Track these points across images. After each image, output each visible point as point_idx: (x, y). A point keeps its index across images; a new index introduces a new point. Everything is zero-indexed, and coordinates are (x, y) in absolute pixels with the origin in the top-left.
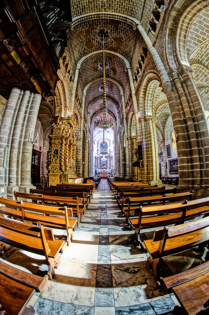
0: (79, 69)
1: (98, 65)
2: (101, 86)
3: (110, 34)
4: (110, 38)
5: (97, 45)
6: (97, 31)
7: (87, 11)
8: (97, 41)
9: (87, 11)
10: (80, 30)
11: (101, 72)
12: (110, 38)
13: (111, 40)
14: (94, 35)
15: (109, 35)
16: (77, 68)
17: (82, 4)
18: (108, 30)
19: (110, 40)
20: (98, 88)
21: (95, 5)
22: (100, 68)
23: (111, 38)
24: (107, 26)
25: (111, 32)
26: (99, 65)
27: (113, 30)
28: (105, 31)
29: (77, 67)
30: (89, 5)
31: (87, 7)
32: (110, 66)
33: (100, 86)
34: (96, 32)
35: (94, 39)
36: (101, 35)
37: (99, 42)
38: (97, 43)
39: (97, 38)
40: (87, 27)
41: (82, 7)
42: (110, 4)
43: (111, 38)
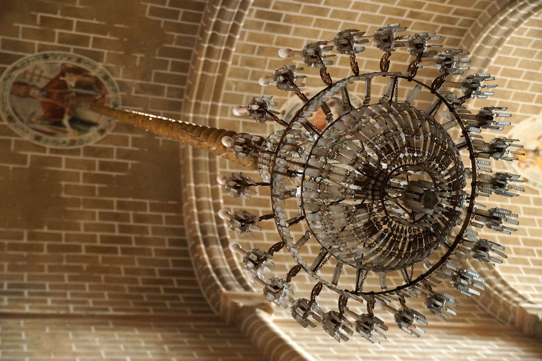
3: (73, 142)
4: (38, 138)
6: (100, 65)
13: (21, 145)
15: (68, 139)
18: (102, 132)
19: (27, 138)
23: (44, 149)
25: (89, 151)
27: (104, 166)
28: (90, 115)
31: (269, 41)
34: (97, 57)
36: (64, 85)
39: (46, 57)
41: (288, 19)
43: (44, 149)
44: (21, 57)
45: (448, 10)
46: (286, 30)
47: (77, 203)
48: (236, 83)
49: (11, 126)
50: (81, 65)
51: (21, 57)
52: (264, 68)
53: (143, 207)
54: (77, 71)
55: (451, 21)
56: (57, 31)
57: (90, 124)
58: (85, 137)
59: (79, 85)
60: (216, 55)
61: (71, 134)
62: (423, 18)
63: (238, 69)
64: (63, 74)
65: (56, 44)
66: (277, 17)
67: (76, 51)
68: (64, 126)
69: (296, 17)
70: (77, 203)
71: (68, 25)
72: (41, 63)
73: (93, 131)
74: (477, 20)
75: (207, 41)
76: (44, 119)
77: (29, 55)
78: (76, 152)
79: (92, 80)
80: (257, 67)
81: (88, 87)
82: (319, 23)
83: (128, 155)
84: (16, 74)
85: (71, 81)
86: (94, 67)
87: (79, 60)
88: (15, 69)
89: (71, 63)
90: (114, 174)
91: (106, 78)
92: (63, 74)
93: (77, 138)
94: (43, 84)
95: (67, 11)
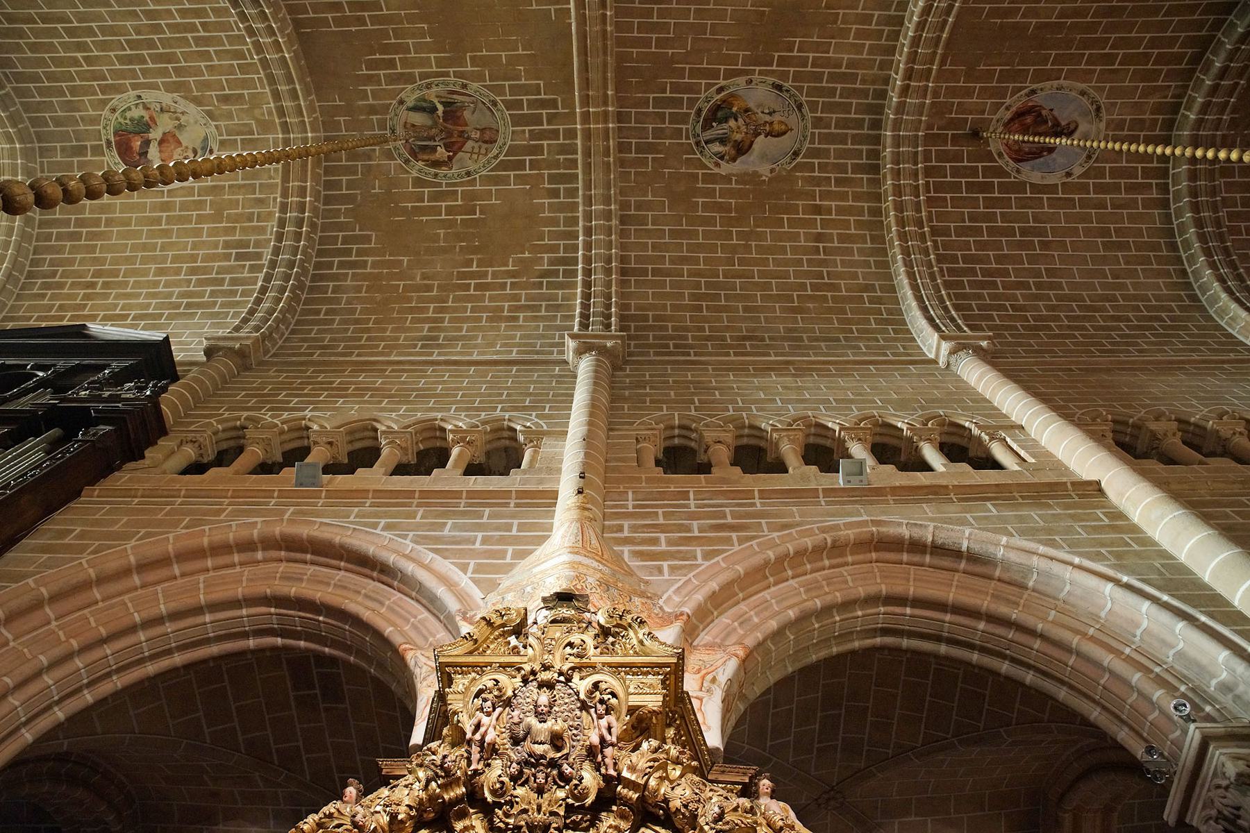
0: (953, 352)
1: (727, 179)
2: (1007, 163)
3: (429, 86)
4: (464, 86)
5: (520, 179)
6: (415, 174)
8: (488, 180)
10: (358, 289)
11: (814, 153)
12: (464, 86)
13: (479, 77)
14: (435, 197)
15: (435, 89)
16: (942, 362)
18: (401, 102)
19: (475, 85)
20: (1020, 187)
21: (240, 187)
22: (764, 157)
23: (456, 75)
24: (372, 110)
25: (410, 79)
26: (726, 168)
27: (391, 64)
28: (419, 119)
29: (935, 362)
30: (229, 219)
31: (243, 229)
32: (730, 74)
33: (1000, 172)
34: (419, 182)
35: (471, 197)
36: (448, 147)
37: (504, 166)
38: (505, 180)
39: (468, 174)
40: (367, 239)
41: (227, 257)
42: (225, 99)
43: (456, 75)
44: (492, 170)
45: (53, 297)
46: (227, 245)
47: (410, 19)
48: (270, 178)
49: (493, 96)
50: (433, 170)
51: (492, 170)
53: (338, 22)
54: (436, 164)
55: (46, 286)
56: (460, 203)
57: (415, 109)
58: (417, 94)
59: (434, 149)
60: (294, 206)
61: (432, 95)
62: (80, 283)
64: (450, 158)
65: (460, 189)
66: (239, 257)
67: (440, 185)
68: (441, 103)
69: (219, 261)
70: (410, 19)
71: (450, 211)
72: (471, 168)
73: (410, 102)
74: (17, 291)
76: (463, 108)
77: (483, 173)
78: (424, 76)
79: (420, 156)
81: (424, 149)
82: (193, 258)
83: (369, 79)
84: (495, 152)
85: (441, 153)
86: (420, 171)
87: (436, 175)
88: (496, 157)
89: (443, 171)
90: (378, 56)
91: (407, 161)
92: (450, 158)
93: (425, 92)
94: (470, 144)
95: (452, 224)
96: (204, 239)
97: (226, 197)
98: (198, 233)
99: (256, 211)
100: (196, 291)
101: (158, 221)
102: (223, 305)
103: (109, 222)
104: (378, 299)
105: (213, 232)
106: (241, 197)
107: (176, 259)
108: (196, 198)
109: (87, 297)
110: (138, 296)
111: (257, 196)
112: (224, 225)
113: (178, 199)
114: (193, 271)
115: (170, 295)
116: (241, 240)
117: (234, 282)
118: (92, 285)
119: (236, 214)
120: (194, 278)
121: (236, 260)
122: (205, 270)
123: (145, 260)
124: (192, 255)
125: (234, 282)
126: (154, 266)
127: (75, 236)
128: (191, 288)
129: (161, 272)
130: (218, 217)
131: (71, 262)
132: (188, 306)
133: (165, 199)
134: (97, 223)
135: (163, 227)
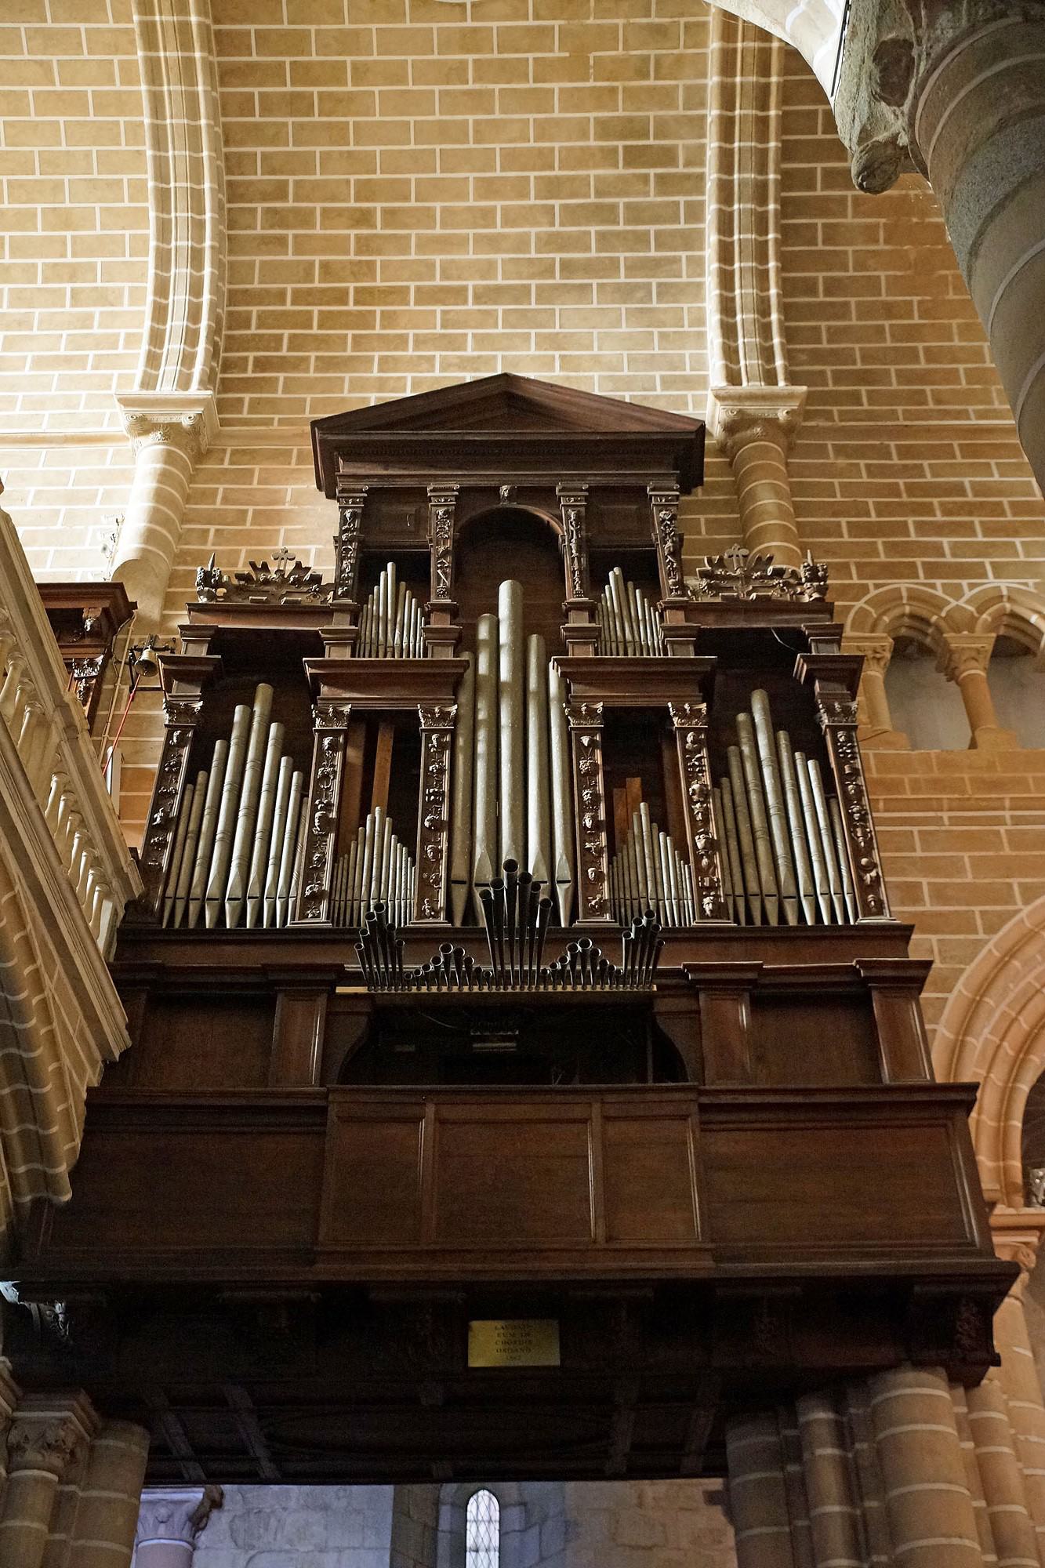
7: (666, 97)
9: (666, 97)
10: (870, 233)
17: (583, 158)
46: (605, 129)
52: (625, 26)
55: (276, 218)
60: (749, 60)
62: (340, 212)
63: (682, 15)
66: (634, 157)
69: (596, 166)
75: (774, 90)
80: (642, 27)
82: (543, 159)
96: (556, 114)
97: (591, 21)
98: (541, 100)
99: (653, 53)
100: (570, 235)
101: (457, 72)
102: (634, 267)
103: (361, 73)
104: (912, 256)
105: (572, 99)
106: (620, 22)
107: (512, 159)
108: (531, 22)
109: (364, 244)
110: (460, 243)
111: (654, 20)
112: (591, 84)
113: (494, 24)
114: (551, 188)
115: (522, 244)
116: (630, 120)
117: (636, 214)
118: (363, 218)
119: (613, 60)
120: (557, 203)
121: (628, 164)
122: (575, 187)
123: (450, 161)
124: (540, 151)
125: (636, 214)
126: (472, 176)
127: (298, 104)
128: (557, 228)
129: (488, 188)
130: (576, 67)
131: (304, 163)
132: (568, 267)
133: (469, 23)
134: (335, 74)
135: (470, 86)
